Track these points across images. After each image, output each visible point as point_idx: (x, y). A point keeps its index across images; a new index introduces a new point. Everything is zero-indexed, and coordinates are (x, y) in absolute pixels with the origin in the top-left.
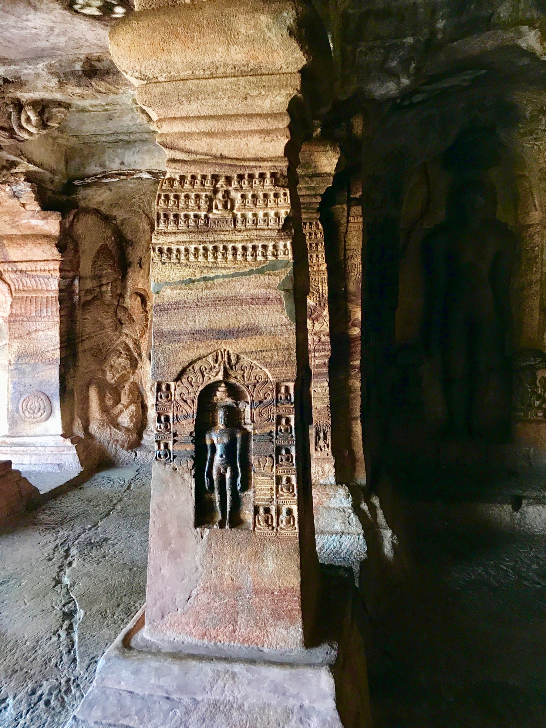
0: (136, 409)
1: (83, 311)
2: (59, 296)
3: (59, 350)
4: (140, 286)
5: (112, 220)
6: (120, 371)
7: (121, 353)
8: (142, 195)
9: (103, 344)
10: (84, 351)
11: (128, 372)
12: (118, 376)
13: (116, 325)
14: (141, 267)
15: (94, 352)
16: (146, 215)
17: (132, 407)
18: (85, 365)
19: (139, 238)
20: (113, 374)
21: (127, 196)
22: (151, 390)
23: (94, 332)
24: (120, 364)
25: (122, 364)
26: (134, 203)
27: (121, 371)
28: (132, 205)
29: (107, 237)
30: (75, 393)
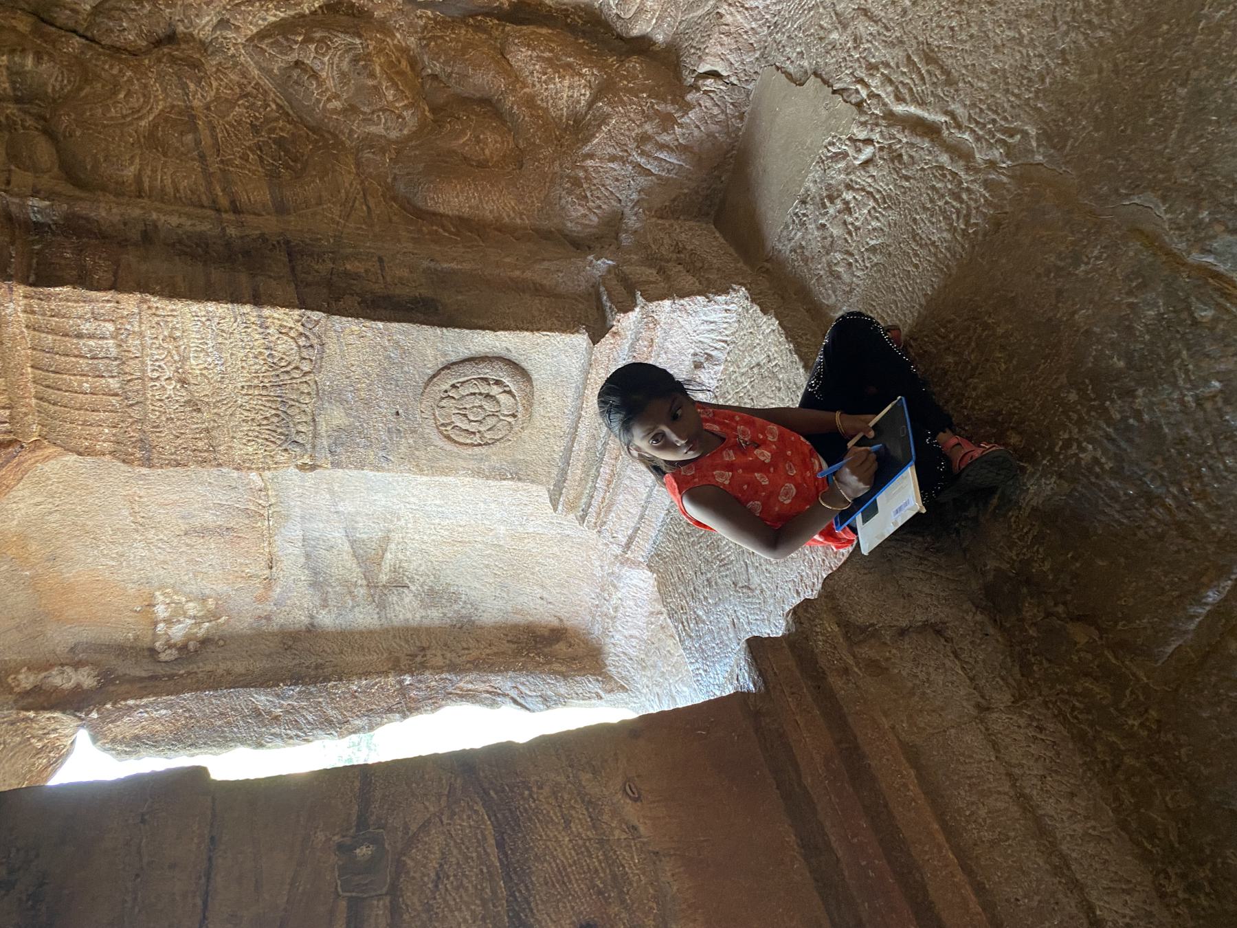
1: (104, 189)
2: (25, 281)
3: (267, 311)
6: (370, 82)
7: (298, 64)
9: (255, 129)
10: (281, 209)
11: (380, 51)
12: (390, 94)
13: (173, 60)
15: (287, 167)
17: (521, 56)
18: (336, 210)
20: (384, 110)
23: (202, 157)
24: (343, 75)
25: (345, 66)
27: (372, 75)
30: (445, 265)
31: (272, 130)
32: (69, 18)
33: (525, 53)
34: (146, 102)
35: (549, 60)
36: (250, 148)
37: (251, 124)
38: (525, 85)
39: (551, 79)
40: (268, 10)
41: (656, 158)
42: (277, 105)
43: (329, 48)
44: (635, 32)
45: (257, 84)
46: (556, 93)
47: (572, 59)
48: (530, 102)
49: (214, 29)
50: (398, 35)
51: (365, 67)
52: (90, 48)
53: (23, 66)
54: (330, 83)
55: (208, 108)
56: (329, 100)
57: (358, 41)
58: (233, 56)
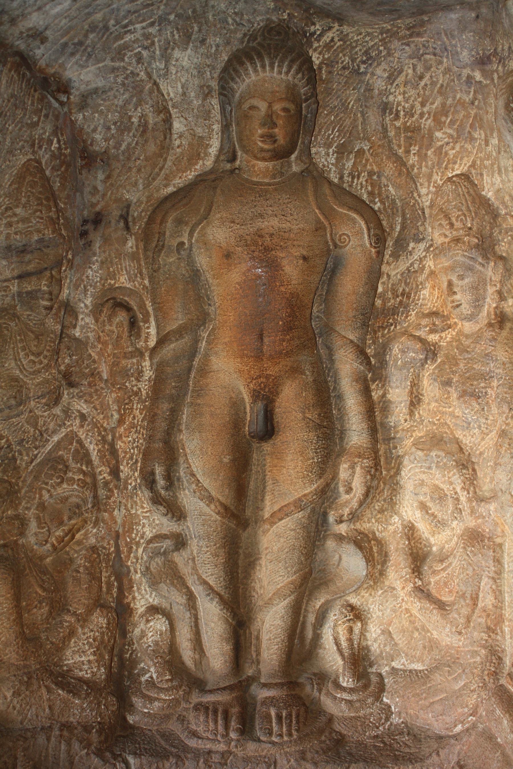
0: (108, 624)
4: (123, 281)
5: (59, 91)
6: (65, 518)
8: (152, 24)
9: (21, 442)
14: (127, 228)
16: (155, 83)
19: (129, 144)
20: (49, 531)
21: (112, 22)
22: (148, 568)
25: (74, 500)
26: (126, 47)
27: (70, 518)
28: (120, 55)
29: (41, 140)
31: (21, 454)
32: (71, 323)
33: (103, 621)
34: (31, 373)
35: (102, 642)
36: (8, 440)
37: (23, 440)
38: (83, 627)
39: (91, 645)
40: (97, 444)
41: (60, 743)
42: (37, 454)
43: (83, 487)
44: (135, 699)
45: (49, 440)
46: (83, 652)
47: (107, 657)
48: (72, 633)
49: (79, 411)
50: (95, 531)
51: (75, 513)
52: (56, 336)
53: (43, 299)
54: (59, 490)
55: (31, 411)
56: (49, 491)
57: (90, 506)
58: (65, 424)
